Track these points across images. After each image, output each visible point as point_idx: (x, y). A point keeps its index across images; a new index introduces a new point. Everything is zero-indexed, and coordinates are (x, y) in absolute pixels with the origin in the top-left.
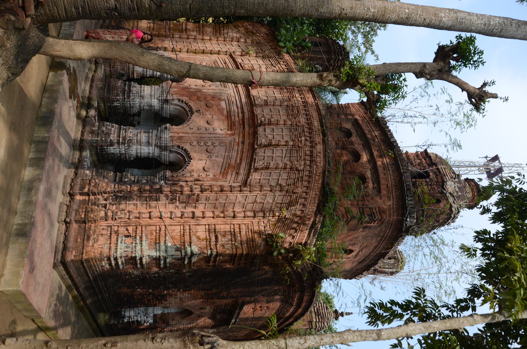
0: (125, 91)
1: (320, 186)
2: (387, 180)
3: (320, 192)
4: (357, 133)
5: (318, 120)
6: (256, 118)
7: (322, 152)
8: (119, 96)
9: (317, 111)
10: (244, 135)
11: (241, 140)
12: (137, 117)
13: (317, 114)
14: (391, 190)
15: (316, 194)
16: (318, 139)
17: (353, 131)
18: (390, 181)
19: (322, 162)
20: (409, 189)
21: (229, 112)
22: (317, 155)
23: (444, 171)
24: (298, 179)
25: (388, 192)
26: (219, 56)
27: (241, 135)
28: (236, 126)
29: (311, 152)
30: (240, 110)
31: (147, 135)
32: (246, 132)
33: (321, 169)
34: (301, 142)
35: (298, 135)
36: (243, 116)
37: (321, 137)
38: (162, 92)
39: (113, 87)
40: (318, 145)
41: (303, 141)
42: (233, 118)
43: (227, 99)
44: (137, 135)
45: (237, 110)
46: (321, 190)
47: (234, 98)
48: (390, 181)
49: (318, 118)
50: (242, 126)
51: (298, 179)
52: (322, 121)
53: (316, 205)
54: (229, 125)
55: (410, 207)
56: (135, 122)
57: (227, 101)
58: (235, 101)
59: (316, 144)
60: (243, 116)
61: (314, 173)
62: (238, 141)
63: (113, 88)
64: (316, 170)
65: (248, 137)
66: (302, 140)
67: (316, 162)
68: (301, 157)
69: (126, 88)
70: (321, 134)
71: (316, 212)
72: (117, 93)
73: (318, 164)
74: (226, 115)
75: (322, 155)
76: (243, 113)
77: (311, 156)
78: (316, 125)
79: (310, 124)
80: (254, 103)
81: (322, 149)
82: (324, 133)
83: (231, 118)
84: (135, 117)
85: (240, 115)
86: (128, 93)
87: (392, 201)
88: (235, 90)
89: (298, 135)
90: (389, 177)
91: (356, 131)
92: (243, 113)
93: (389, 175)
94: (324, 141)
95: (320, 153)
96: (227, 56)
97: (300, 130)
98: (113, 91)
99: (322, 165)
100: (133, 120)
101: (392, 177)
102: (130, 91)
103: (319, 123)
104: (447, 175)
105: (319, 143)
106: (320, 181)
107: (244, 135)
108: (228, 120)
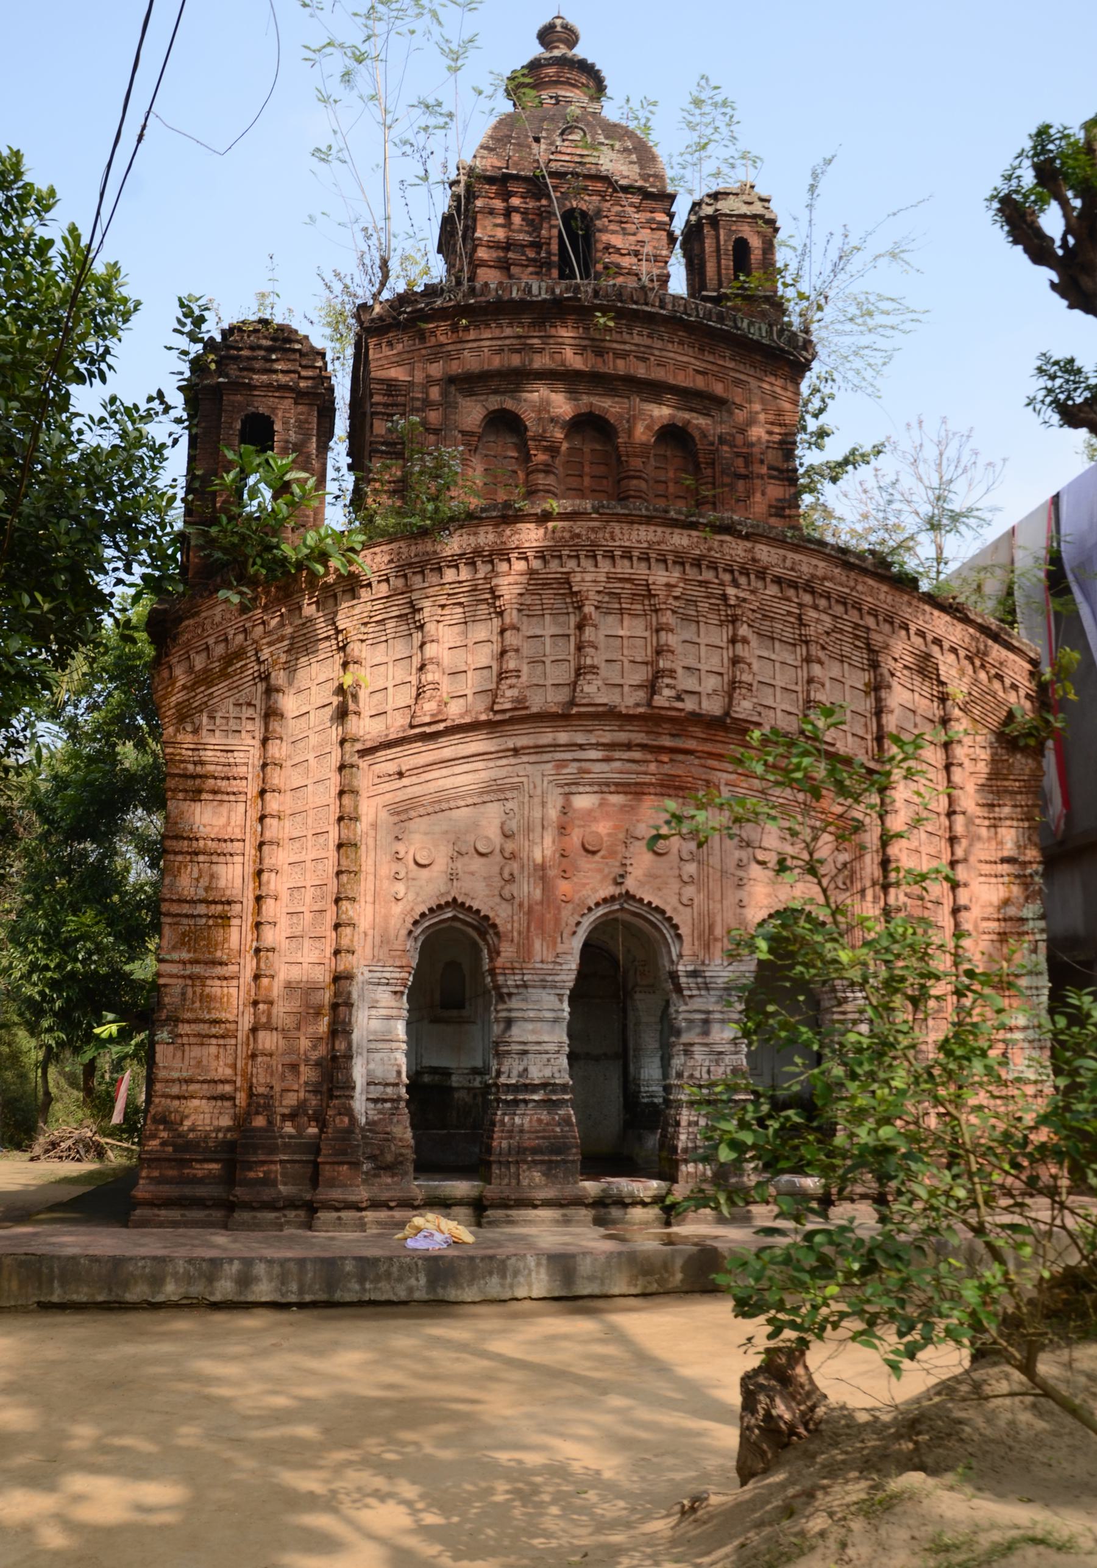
0: (550, 1100)
1: (885, 588)
2: (684, 367)
3: (902, 591)
4: (504, 393)
5: (668, 530)
6: (663, 712)
7: (782, 552)
8: (569, 1116)
9: (632, 523)
10: (711, 755)
11: (730, 767)
12: (454, 1078)
13: (643, 528)
14: (715, 368)
15: (910, 604)
16: (736, 550)
17: (494, 402)
18: (685, 359)
19: (815, 562)
20: (721, 318)
21: (620, 789)
22: (792, 569)
23: (567, 158)
24: (857, 637)
25: (720, 380)
26: (364, 794)
27: (711, 762)
28: (680, 773)
29: (778, 581)
30: (617, 755)
31: (715, 1028)
32: (706, 749)
33: (837, 570)
34: (744, 600)
35: (713, 601)
36: (643, 747)
37: (728, 538)
38: (544, 987)
39: (538, 1138)
40: (758, 556)
41: (742, 595)
42: (647, 779)
43: (567, 789)
44: (721, 1053)
45: (617, 765)
46: (897, 589)
47: (566, 766)
48: (685, 359)
49: (659, 530)
50: (680, 757)
51: (857, 637)
52: (672, 519)
53: (936, 613)
54: (671, 792)
55: (779, 337)
56: (477, 1084)
57: (574, 789)
58: (576, 765)
59: (754, 560)
60: (643, 747)
61: (847, 590)
62: (734, 776)
63: (544, 1138)
64: (842, 585)
65: (720, 745)
66: (737, 597)
67: (813, 576)
68: (789, 613)
69: (536, 1097)
70: (718, 537)
71: (955, 617)
72: (559, 1125)
73: (820, 573)
74: (629, 797)
75: (790, 555)
76: (628, 746)
77: (794, 585)
78: (685, 542)
79: (680, 559)
80: (601, 709)
81: (773, 550)
82: (719, 527)
83: (644, 784)
84: (455, 1085)
85: (637, 755)
86: (554, 1092)
87: (750, 379)
88: (525, 759)
89: (713, 601)
90: (671, 355)
91: (496, 392)
92: (628, 746)
93: (665, 353)
94: (747, 537)
95: (784, 561)
96: (363, 764)
97: (697, 592)
98: (555, 1137)
99: (822, 564)
100: (469, 1089)
101: (670, 346)
102: (544, 1086)
103: (677, 531)
104: (582, 156)
105: (751, 550)
106: (870, 582)
107: (711, 755)
108: (644, 794)
